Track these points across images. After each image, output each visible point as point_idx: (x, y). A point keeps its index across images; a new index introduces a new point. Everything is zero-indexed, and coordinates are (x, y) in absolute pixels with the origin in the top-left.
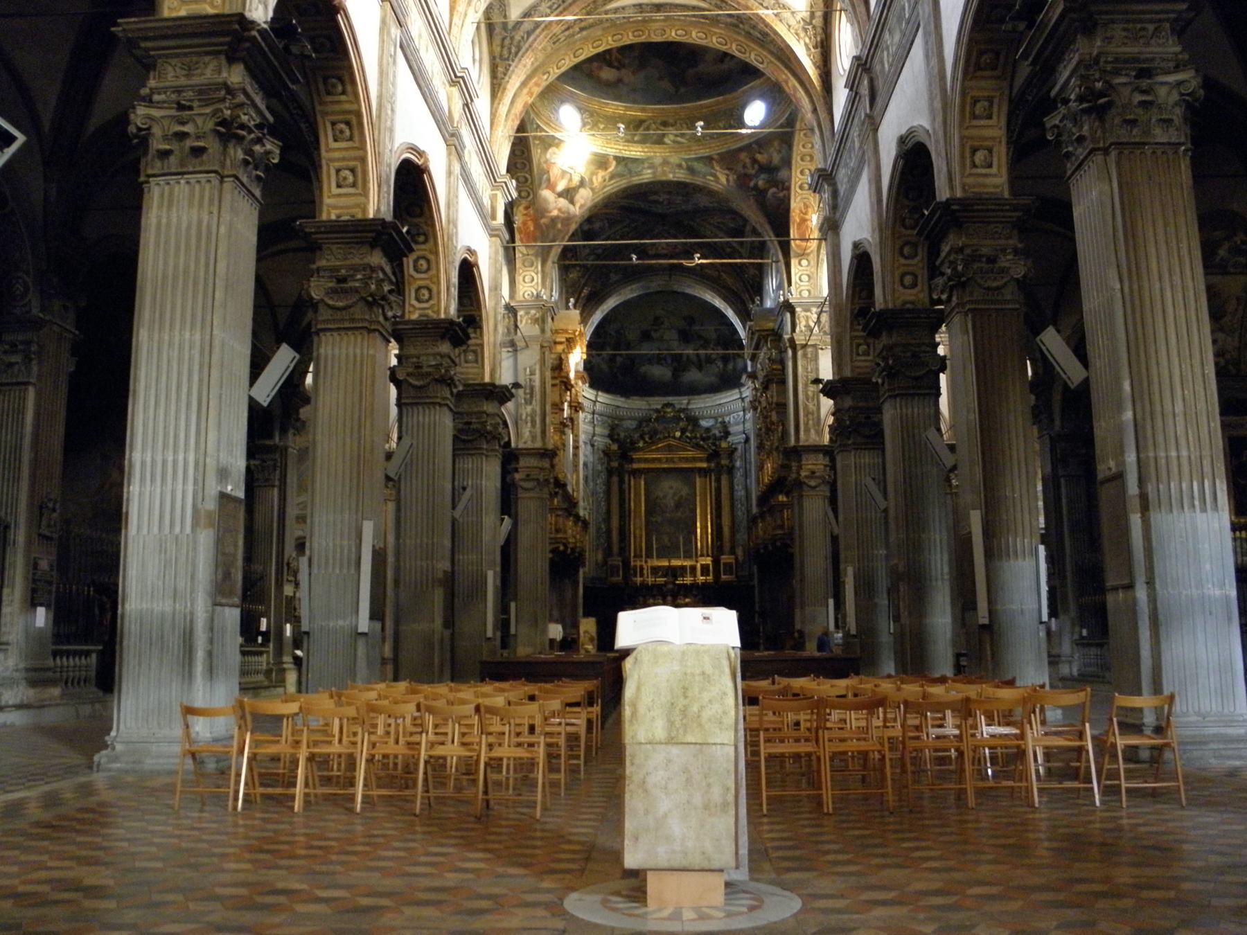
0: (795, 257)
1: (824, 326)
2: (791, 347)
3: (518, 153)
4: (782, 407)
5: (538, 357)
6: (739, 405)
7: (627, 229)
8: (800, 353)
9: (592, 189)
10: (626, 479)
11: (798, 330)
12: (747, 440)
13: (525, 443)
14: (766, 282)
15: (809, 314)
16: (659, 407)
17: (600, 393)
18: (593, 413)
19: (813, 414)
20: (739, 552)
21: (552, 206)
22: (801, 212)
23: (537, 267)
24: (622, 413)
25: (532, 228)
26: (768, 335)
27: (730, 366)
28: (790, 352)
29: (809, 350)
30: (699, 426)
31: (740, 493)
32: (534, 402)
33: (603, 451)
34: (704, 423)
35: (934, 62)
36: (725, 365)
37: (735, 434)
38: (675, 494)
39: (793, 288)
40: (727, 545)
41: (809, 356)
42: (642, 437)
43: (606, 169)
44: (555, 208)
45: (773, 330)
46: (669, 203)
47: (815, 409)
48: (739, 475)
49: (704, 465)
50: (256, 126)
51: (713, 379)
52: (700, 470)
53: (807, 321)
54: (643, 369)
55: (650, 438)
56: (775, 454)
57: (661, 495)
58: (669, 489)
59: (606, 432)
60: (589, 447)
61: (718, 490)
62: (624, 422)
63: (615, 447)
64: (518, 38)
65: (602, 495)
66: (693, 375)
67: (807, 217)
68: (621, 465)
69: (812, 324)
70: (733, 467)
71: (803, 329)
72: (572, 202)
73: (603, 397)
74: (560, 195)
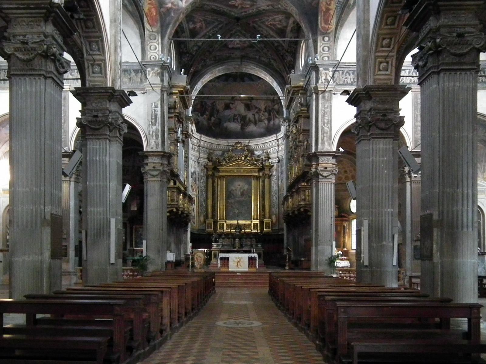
0: (321, 35)
2: (315, 93)
4: (307, 132)
5: (159, 97)
6: (276, 143)
7: (216, 29)
8: (320, 96)
10: (216, 181)
11: (320, 82)
13: (152, 148)
14: (297, 61)
15: (327, 72)
16: (234, 144)
17: (202, 136)
18: (199, 146)
19: (327, 133)
22: (327, 3)
23: (158, 40)
24: (214, 147)
25: (155, 14)
26: (299, 90)
27: (272, 123)
28: (314, 96)
29: (327, 94)
31: (275, 188)
32: (157, 124)
33: (204, 166)
34: (257, 153)
36: (269, 122)
37: (273, 158)
38: (240, 189)
40: (267, 215)
41: (326, 98)
42: (224, 159)
45: (303, 87)
46: (242, 8)
47: (329, 131)
48: (274, 179)
49: (257, 174)
51: (262, 130)
52: (254, 176)
53: (326, 76)
54: (225, 125)
55: (229, 160)
56: (301, 159)
57: (234, 189)
58: (239, 186)
59: (206, 156)
60: (197, 164)
61: (264, 186)
62: (215, 151)
63: (210, 164)
65: (203, 188)
67: (330, 7)
68: (213, 173)
69: (329, 78)
70: (271, 175)
71: (323, 81)
73: (204, 138)
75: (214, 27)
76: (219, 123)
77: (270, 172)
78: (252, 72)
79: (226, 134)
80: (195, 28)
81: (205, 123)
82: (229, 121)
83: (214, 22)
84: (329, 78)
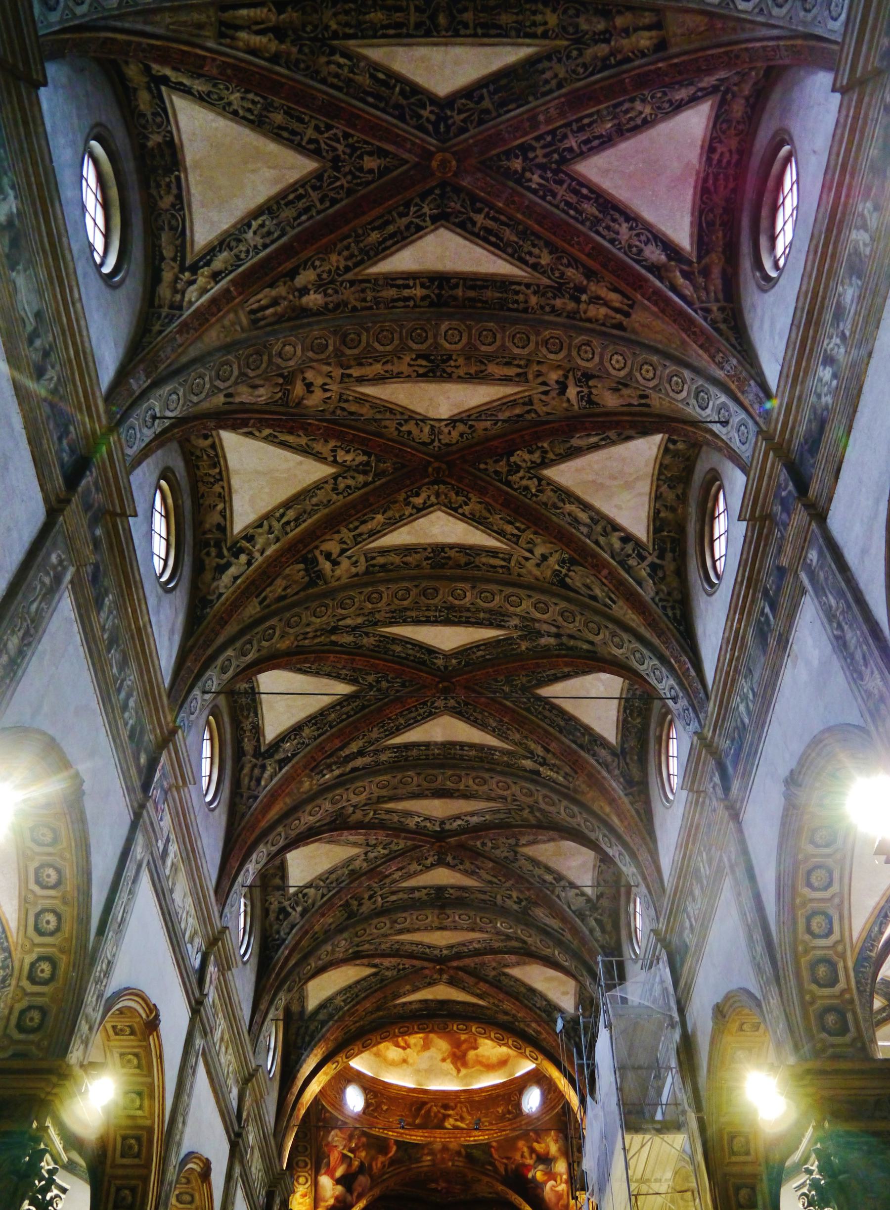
9: (371, 1176)
43: (386, 1154)
64: (312, 1027)
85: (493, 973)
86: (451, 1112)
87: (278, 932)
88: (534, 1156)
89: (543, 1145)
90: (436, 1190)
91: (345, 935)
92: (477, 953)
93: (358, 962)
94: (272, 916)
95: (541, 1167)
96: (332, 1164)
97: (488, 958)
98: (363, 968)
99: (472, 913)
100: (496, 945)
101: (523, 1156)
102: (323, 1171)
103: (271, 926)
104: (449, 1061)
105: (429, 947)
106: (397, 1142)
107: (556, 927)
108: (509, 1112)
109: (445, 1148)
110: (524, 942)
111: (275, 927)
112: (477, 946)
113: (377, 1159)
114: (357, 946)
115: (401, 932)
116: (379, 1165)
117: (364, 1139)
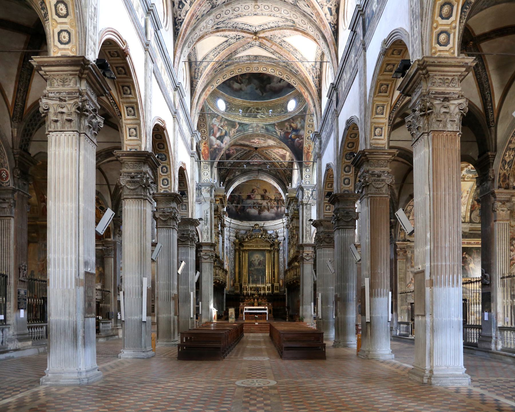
1: (314, 196)
3: (201, 120)
12: (284, 239)
20: (281, 282)
21: (214, 143)
30: (267, 233)
31: (281, 259)
34: (269, 232)
35: (363, 88)
39: (303, 181)
44: (216, 144)
45: (295, 197)
48: (281, 252)
49: (269, 248)
50: (92, 110)
52: (268, 250)
53: (308, 194)
54: (248, 210)
61: (274, 258)
66: (266, 213)
69: (310, 196)
70: (279, 249)
72: (222, 142)
74: (218, 139)
75: (242, 153)
76: (243, 209)
77: (279, 247)
78: (265, 180)
79: (248, 218)
80: (229, 153)
81: (234, 209)
82: (250, 207)
83: (241, 150)
84: (310, 196)
85: (279, 41)
86: (260, 111)
87: (180, 16)
88: (291, 129)
89: (295, 124)
90: (254, 142)
91: (211, 17)
92: (272, 29)
93: (218, 34)
94: (176, 6)
95: (294, 133)
96: (215, 132)
97: (276, 32)
98: (221, 38)
99: (270, 5)
100: (281, 24)
101: (287, 129)
102: (211, 135)
103: (176, 12)
104: (258, 89)
105: (250, 26)
106: (239, 123)
107: (309, 13)
108: (283, 111)
109: (258, 126)
110: (294, 22)
111: (179, 12)
112: (272, 25)
113: (231, 130)
114: (217, 24)
115: (237, 17)
116: (233, 132)
117: (226, 122)
